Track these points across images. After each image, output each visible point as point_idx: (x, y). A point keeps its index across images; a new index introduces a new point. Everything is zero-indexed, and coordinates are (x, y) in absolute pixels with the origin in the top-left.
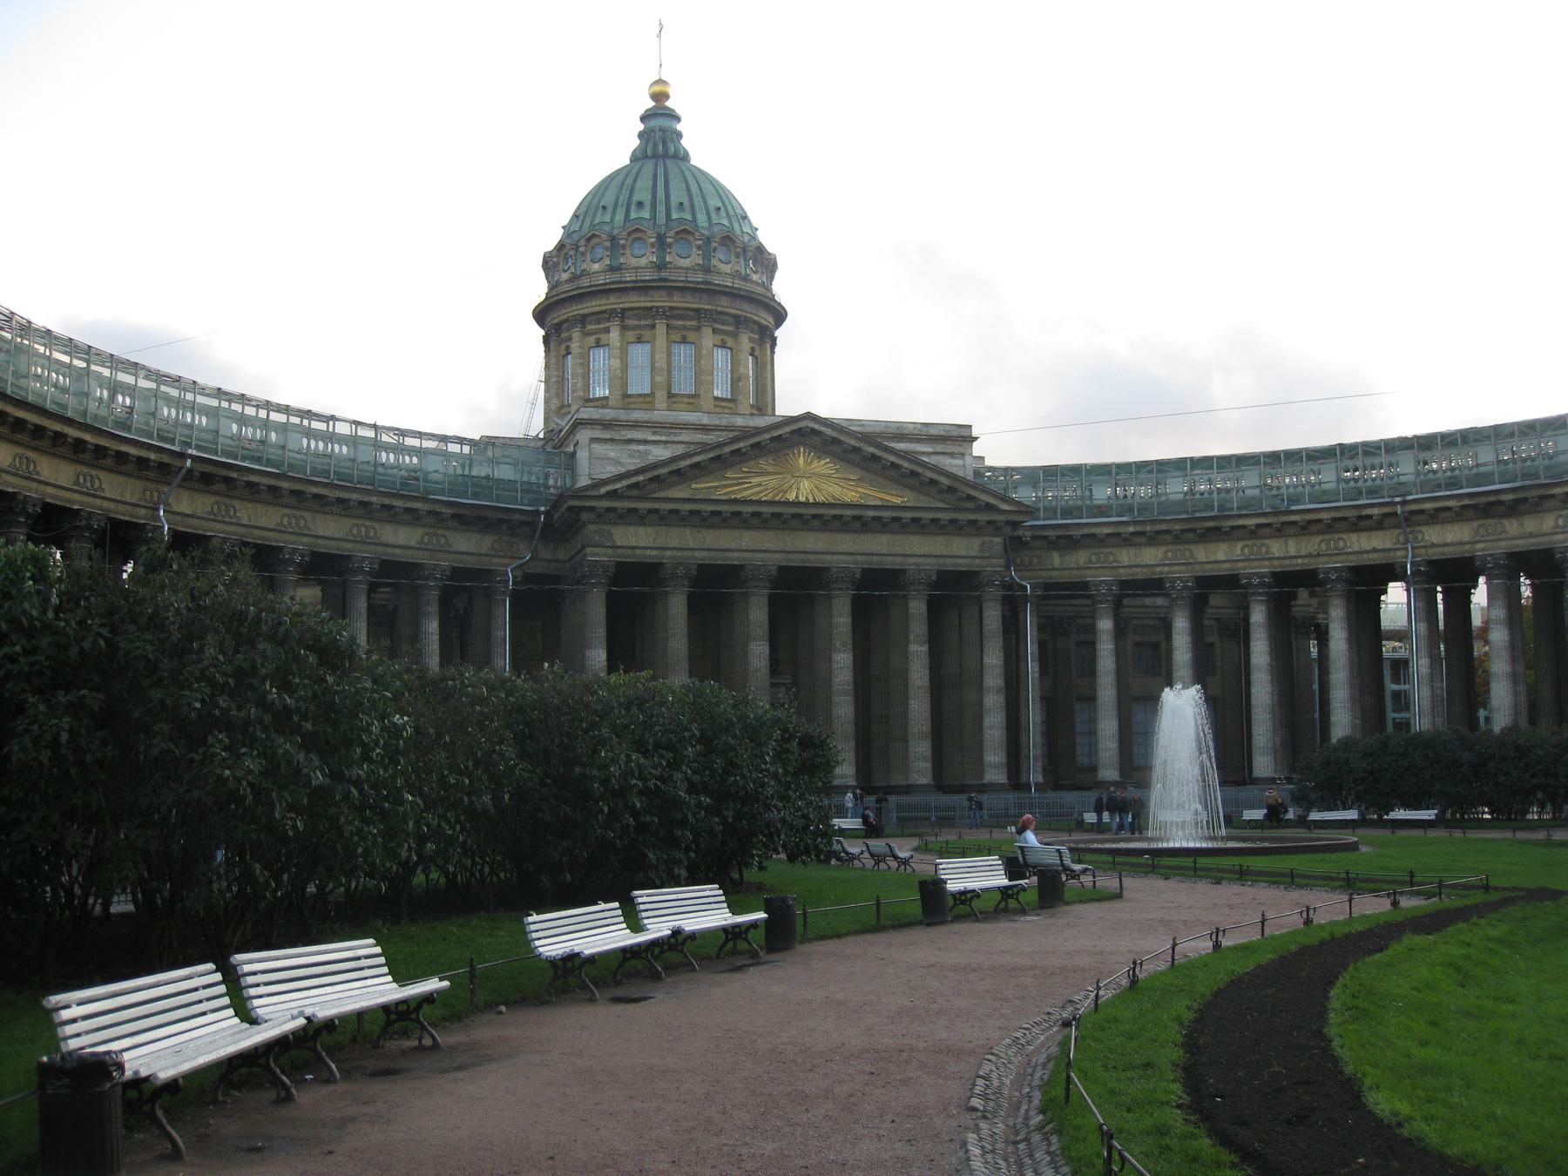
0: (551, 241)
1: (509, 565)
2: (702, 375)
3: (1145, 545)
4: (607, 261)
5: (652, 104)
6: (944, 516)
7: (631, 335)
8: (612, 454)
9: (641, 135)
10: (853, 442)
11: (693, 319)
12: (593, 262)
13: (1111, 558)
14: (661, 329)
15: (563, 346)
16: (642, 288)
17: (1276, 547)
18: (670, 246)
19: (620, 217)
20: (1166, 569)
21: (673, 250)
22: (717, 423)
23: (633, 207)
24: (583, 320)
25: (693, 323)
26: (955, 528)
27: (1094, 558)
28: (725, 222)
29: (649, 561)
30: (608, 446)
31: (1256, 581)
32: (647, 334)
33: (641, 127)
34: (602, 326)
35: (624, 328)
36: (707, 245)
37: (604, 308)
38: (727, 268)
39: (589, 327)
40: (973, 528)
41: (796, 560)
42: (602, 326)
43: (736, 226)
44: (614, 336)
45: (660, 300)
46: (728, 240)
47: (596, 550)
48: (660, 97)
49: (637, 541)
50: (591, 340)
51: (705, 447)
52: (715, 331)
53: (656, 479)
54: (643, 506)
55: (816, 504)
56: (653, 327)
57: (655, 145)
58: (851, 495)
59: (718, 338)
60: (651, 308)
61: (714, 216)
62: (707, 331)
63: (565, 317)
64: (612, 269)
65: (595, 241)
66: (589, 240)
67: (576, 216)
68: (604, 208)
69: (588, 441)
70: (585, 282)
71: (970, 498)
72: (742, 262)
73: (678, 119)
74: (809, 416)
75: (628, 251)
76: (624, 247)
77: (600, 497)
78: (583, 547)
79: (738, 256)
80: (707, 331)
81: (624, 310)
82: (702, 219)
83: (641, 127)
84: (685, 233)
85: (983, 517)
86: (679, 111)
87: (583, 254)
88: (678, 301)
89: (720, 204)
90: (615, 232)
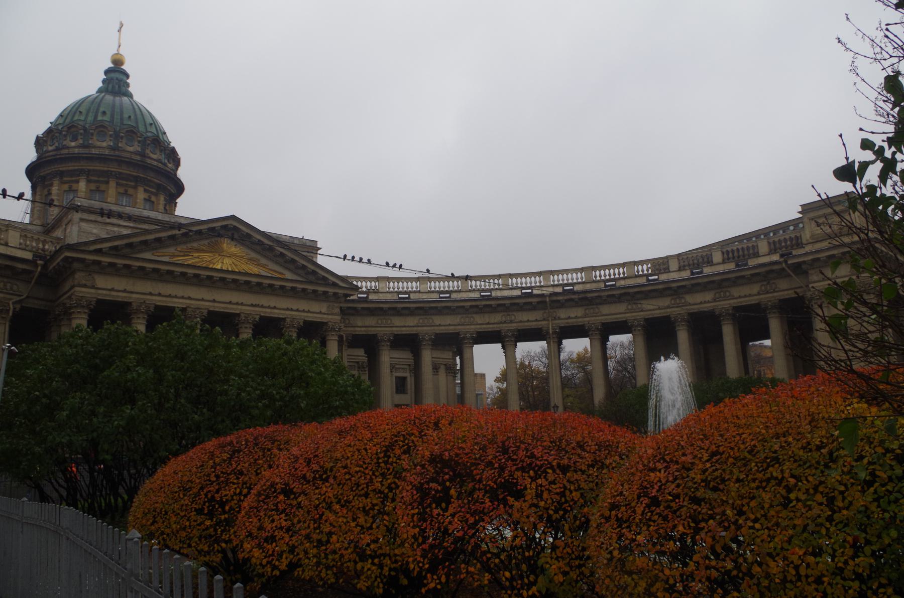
0: (41, 128)
1: (10, 299)
3: (408, 315)
4: (81, 141)
5: (112, 65)
6: (310, 287)
7: (93, 186)
8: (95, 231)
9: (104, 81)
11: (131, 181)
12: (71, 141)
13: (389, 322)
14: (112, 184)
15: (46, 190)
16: (102, 159)
17: (479, 319)
18: (122, 138)
19: (90, 118)
20: (419, 328)
21: (124, 141)
22: (168, 220)
23: (100, 114)
24: (61, 174)
25: (133, 184)
26: (315, 296)
27: (380, 322)
29: (120, 300)
30: (92, 225)
31: (468, 336)
32: (103, 187)
34: (74, 179)
35: (89, 181)
36: (144, 143)
37: (76, 168)
38: (154, 157)
39: (65, 179)
40: (323, 297)
41: (218, 308)
42: (74, 179)
43: (160, 135)
44: (82, 185)
45: (113, 168)
47: (83, 289)
48: (118, 62)
50: (66, 187)
52: (145, 190)
53: (130, 245)
54: (120, 262)
55: (233, 272)
56: (107, 183)
57: (113, 87)
58: (255, 270)
59: (146, 196)
60: (109, 171)
61: (148, 127)
62: (141, 190)
63: (49, 172)
64: (83, 146)
65: (73, 130)
66: (69, 128)
67: (61, 115)
68: (81, 112)
69: (78, 220)
70: (66, 151)
71: (324, 278)
72: (163, 156)
73: (128, 76)
74: (233, 217)
75: (95, 138)
76: (92, 134)
77: (90, 252)
78: (73, 287)
79: (161, 151)
80: (141, 190)
81: (89, 170)
82: (141, 128)
84: (132, 133)
85: (331, 290)
86: (128, 71)
87: (65, 136)
88: (125, 170)
89: (152, 122)
90: (87, 126)
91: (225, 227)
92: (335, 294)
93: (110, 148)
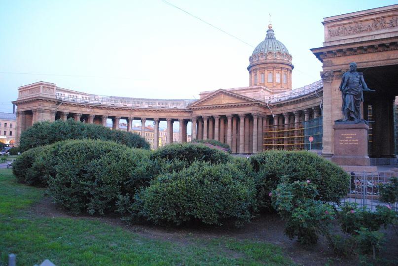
2: (274, 79)
9: (267, 35)
10: (228, 93)
14: (258, 72)
28: (271, 49)
33: (267, 33)
38: (271, 58)
41: (221, 114)
43: (274, 50)
45: (258, 67)
46: (270, 53)
49: (199, 113)
51: (205, 97)
54: (198, 107)
59: (269, 72)
62: (266, 71)
71: (248, 100)
74: (221, 89)
80: (266, 71)
82: (266, 50)
83: (267, 33)
85: (250, 103)
91: (220, 92)
92: (252, 104)
93: (258, 61)
